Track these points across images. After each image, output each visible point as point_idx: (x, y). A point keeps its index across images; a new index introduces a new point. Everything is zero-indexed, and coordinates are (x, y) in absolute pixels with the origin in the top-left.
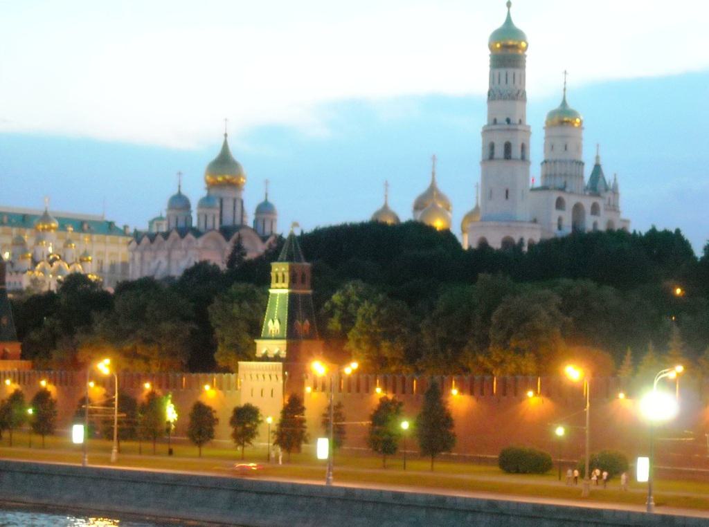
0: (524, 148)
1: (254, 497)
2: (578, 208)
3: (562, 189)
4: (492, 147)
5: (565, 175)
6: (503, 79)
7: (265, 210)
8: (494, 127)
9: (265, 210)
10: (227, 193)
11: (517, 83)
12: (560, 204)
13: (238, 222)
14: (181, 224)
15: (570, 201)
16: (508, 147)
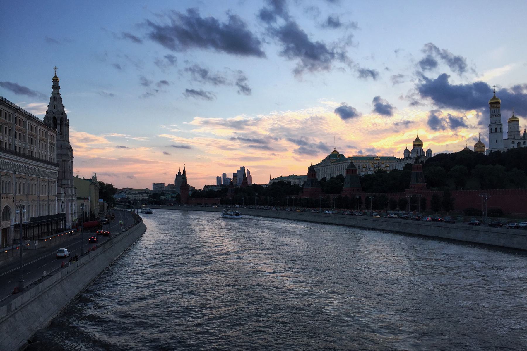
0: (500, 129)
3: (514, 139)
4: (491, 129)
5: (515, 135)
6: (493, 112)
7: (429, 151)
8: (492, 124)
9: (429, 151)
10: (418, 148)
11: (498, 112)
12: (513, 142)
13: (422, 155)
14: (407, 156)
15: (516, 142)
16: (496, 129)
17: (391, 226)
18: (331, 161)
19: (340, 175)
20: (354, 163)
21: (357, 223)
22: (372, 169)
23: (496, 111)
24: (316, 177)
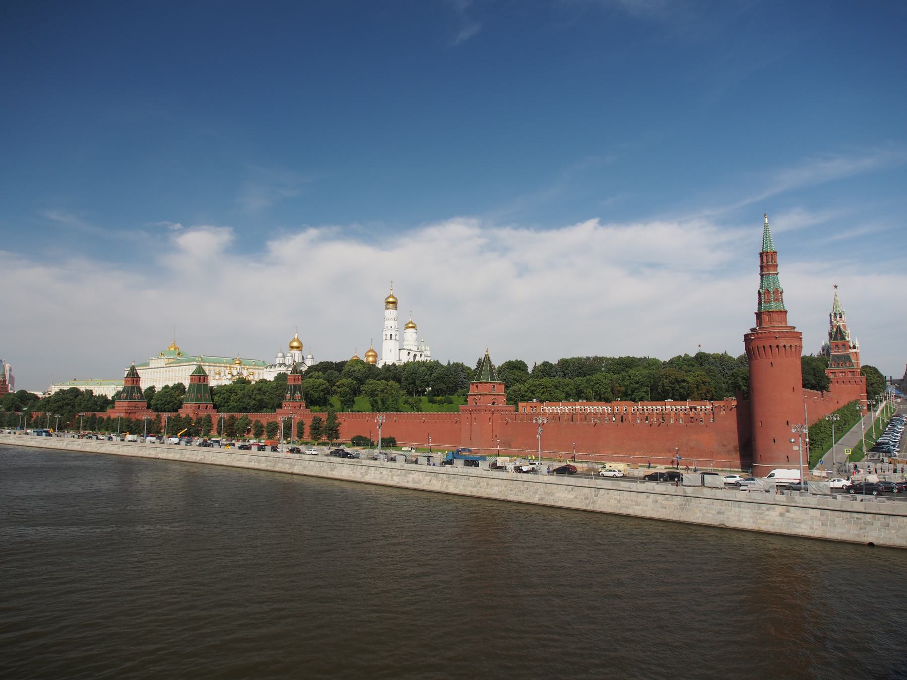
1: (257, 457)
2: (415, 356)
6: (389, 314)
14: (281, 362)
17: (255, 462)
18: (166, 360)
19: (178, 384)
20: (204, 367)
21: (202, 457)
22: (230, 376)
23: (392, 312)
24: (139, 385)
